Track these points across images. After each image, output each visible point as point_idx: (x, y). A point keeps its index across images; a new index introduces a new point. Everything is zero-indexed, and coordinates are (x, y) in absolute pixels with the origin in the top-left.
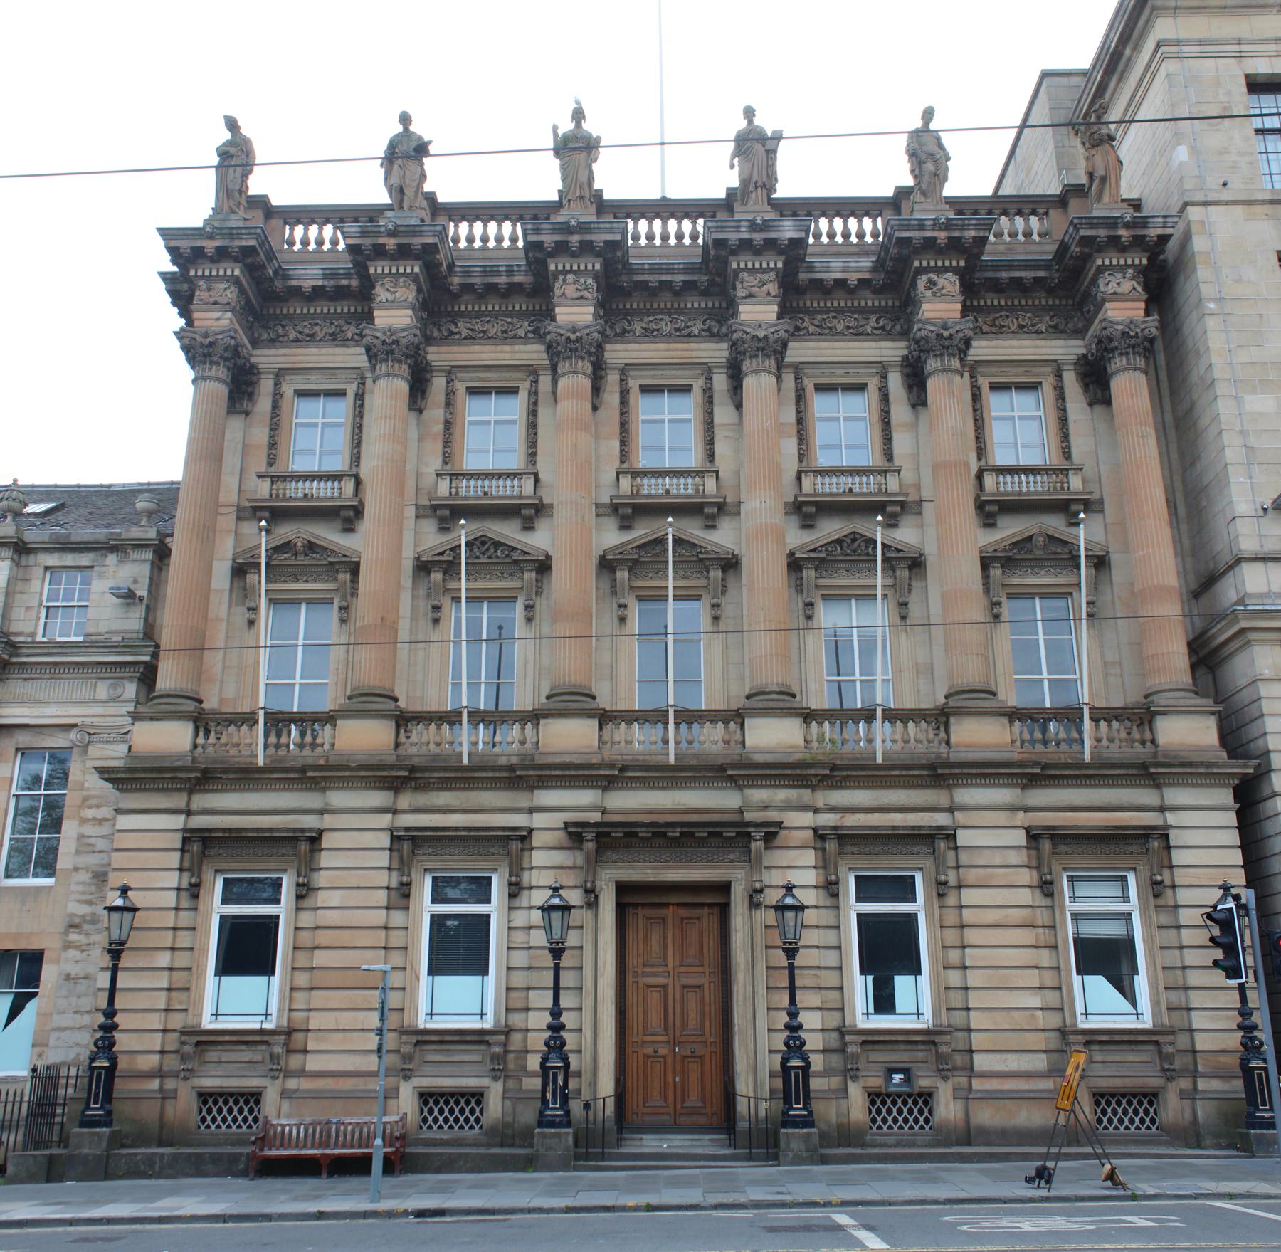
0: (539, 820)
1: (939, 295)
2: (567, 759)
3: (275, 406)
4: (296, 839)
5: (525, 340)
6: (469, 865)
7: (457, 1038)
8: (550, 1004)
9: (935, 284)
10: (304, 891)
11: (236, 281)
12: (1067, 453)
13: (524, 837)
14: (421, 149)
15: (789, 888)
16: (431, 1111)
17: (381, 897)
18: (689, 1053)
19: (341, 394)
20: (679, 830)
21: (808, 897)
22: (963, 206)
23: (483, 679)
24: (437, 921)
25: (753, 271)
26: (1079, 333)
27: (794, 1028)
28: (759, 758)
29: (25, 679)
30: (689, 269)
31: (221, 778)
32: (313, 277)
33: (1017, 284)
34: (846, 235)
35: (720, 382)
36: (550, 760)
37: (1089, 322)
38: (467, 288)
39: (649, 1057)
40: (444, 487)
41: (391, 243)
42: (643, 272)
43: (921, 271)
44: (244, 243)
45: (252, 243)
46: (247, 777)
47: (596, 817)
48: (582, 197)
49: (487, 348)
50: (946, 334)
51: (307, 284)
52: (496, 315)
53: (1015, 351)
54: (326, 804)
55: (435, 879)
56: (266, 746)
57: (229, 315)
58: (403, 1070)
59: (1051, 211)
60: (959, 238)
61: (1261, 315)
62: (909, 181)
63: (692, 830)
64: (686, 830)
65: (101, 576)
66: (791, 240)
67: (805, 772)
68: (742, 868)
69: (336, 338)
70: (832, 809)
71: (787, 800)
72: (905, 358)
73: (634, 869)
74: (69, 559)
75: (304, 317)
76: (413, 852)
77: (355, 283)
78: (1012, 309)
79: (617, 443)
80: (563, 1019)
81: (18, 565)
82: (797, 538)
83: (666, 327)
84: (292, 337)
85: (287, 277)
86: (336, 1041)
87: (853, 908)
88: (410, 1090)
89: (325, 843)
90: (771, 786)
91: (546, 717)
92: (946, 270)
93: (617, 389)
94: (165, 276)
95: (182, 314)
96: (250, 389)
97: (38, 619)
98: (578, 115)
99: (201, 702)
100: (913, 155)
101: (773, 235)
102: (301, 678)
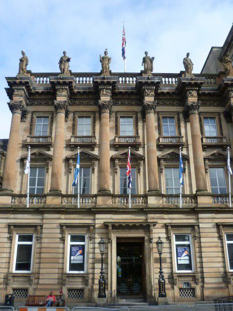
1: (192, 96)
3: (32, 120)
5: (92, 105)
8: (101, 267)
9: (191, 93)
10: (39, 239)
12: (222, 134)
14: (68, 60)
15: (159, 238)
16: (70, 294)
19: (48, 117)
21: (164, 240)
22: (196, 75)
25: (148, 89)
26: (224, 106)
27: (161, 272)
28: (151, 206)
30: (132, 89)
34: (169, 82)
35: (139, 115)
37: (226, 104)
40: (73, 140)
43: (188, 90)
44: (26, 81)
51: (40, 91)
52: (86, 99)
56: (29, 202)
59: (216, 78)
62: (184, 70)
69: (47, 104)
70: (169, 219)
72: (184, 111)
75: (39, 99)
77: (52, 91)
82: (159, 154)
83: (126, 102)
85: (35, 89)
86: (47, 276)
87: (175, 243)
89: (44, 227)
91: (98, 196)
94: (6, 89)
95: (9, 98)
98: (106, 53)
99: (13, 191)
100: (184, 63)
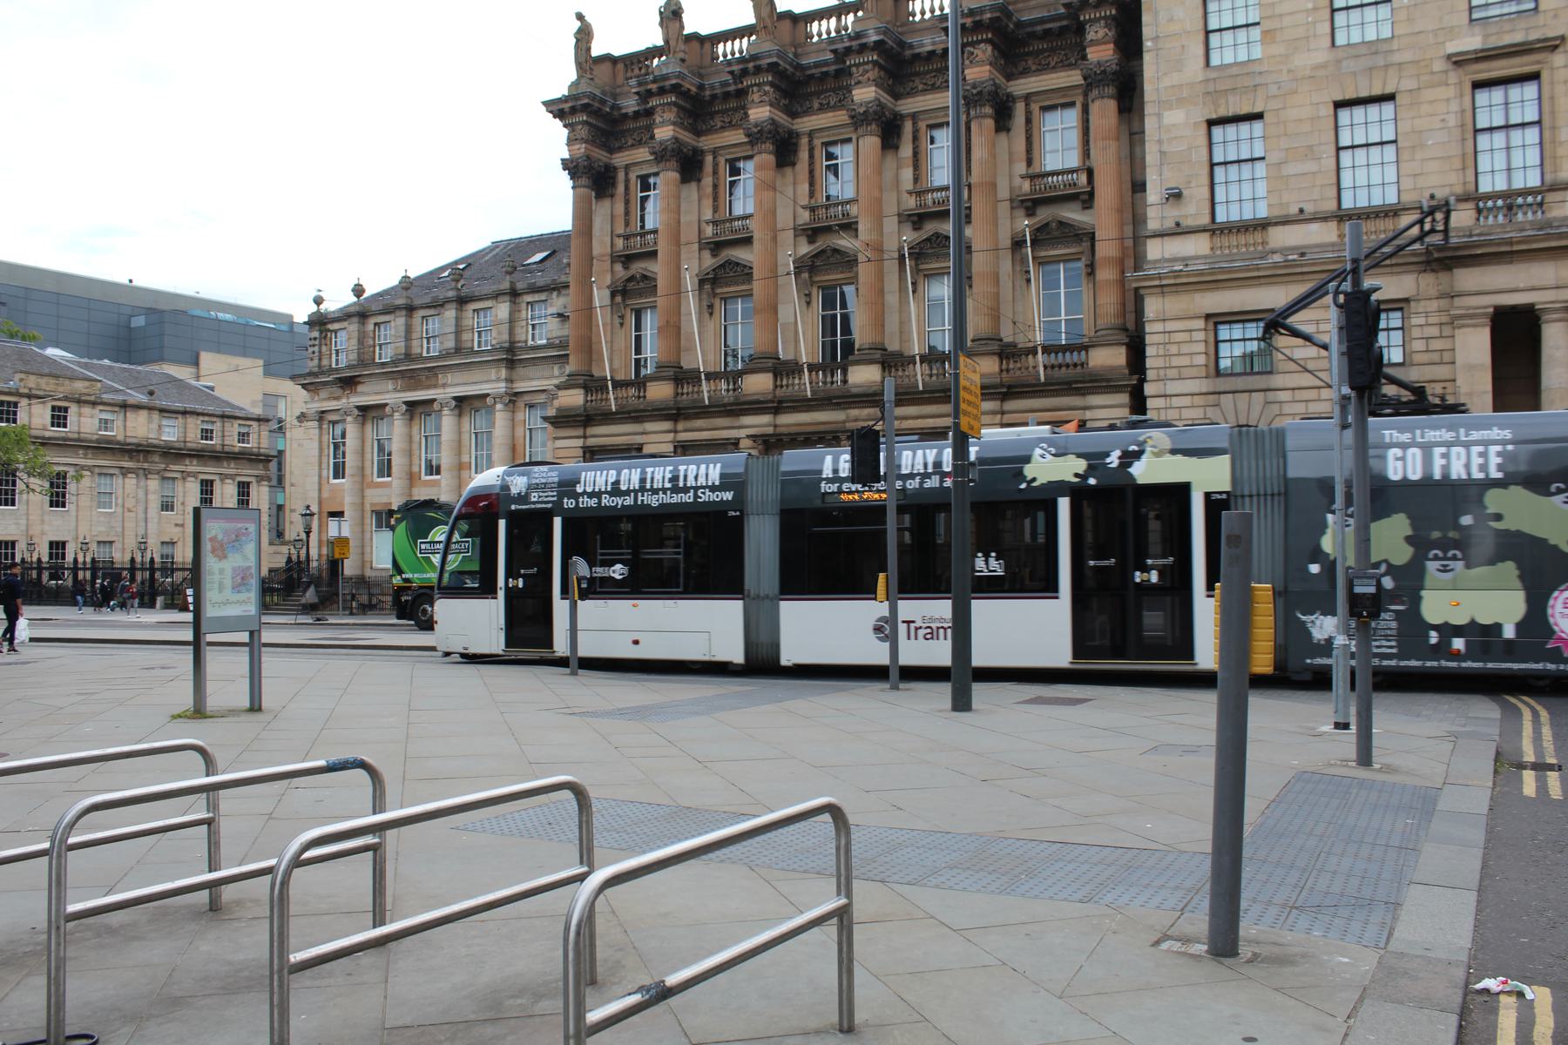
0: (742, 433)
2: (755, 397)
11: (585, 123)
28: (854, 391)
32: (632, 106)
33: (1047, 32)
38: (714, 97)
41: (654, 87)
42: (810, 68)
45: (586, 101)
46: (607, 418)
47: (770, 430)
48: (765, 27)
49: (733, 132)
50: (975, 91)
51: (630, 110)
53: (1054, 81)
57: (584, 145)
60: (981, 21)
61: (1183, 46)
65: (551, 305)
66: (875, 42)
71: (869, 415)
74: (536, 297)
75: (634, 130)
78: (1053, 50)
79: (806, 186)
81: (515, 303)
84: (629, 144)
90: (858, 408)
91: (746, 373)
92: (979, 42)
93: (807, 148)
96: (611, 181)
97: (527, 332)
101: (864, 41)
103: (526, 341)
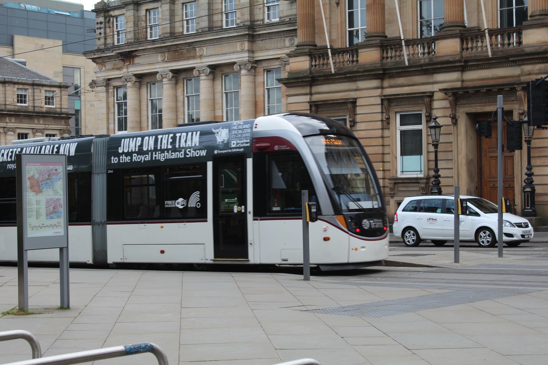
0: (436, 87)
2: (446, 58)
4: (346, 102)
6: (411, 109)
7: (408, 181)
13: (431, 96)
17: (379, 125)
18: (507, 186)
20: (485, 89)
23: (433, 18)
24: (403, 133)
28: (528, 50)
29: (262, 40)
31: (318, 79)
36: (442, 59)
39: (491, 187)
46: (328, 78)
47: (458, 84)
54: (357, 87)
55: (401, 115)
58: (390, 194)
63: (491, 88)
64: (488, 88)
67: (544, 56)
68: (517, 104)
71: (540, 69)
73: (472, 107)
76: (389, 105)
80: (439, 173)
88: (394, 201)
89: (358, 104)
91: (438, 39)
97: (264, 12)
102: (361, 26)
103: (263, 20)
